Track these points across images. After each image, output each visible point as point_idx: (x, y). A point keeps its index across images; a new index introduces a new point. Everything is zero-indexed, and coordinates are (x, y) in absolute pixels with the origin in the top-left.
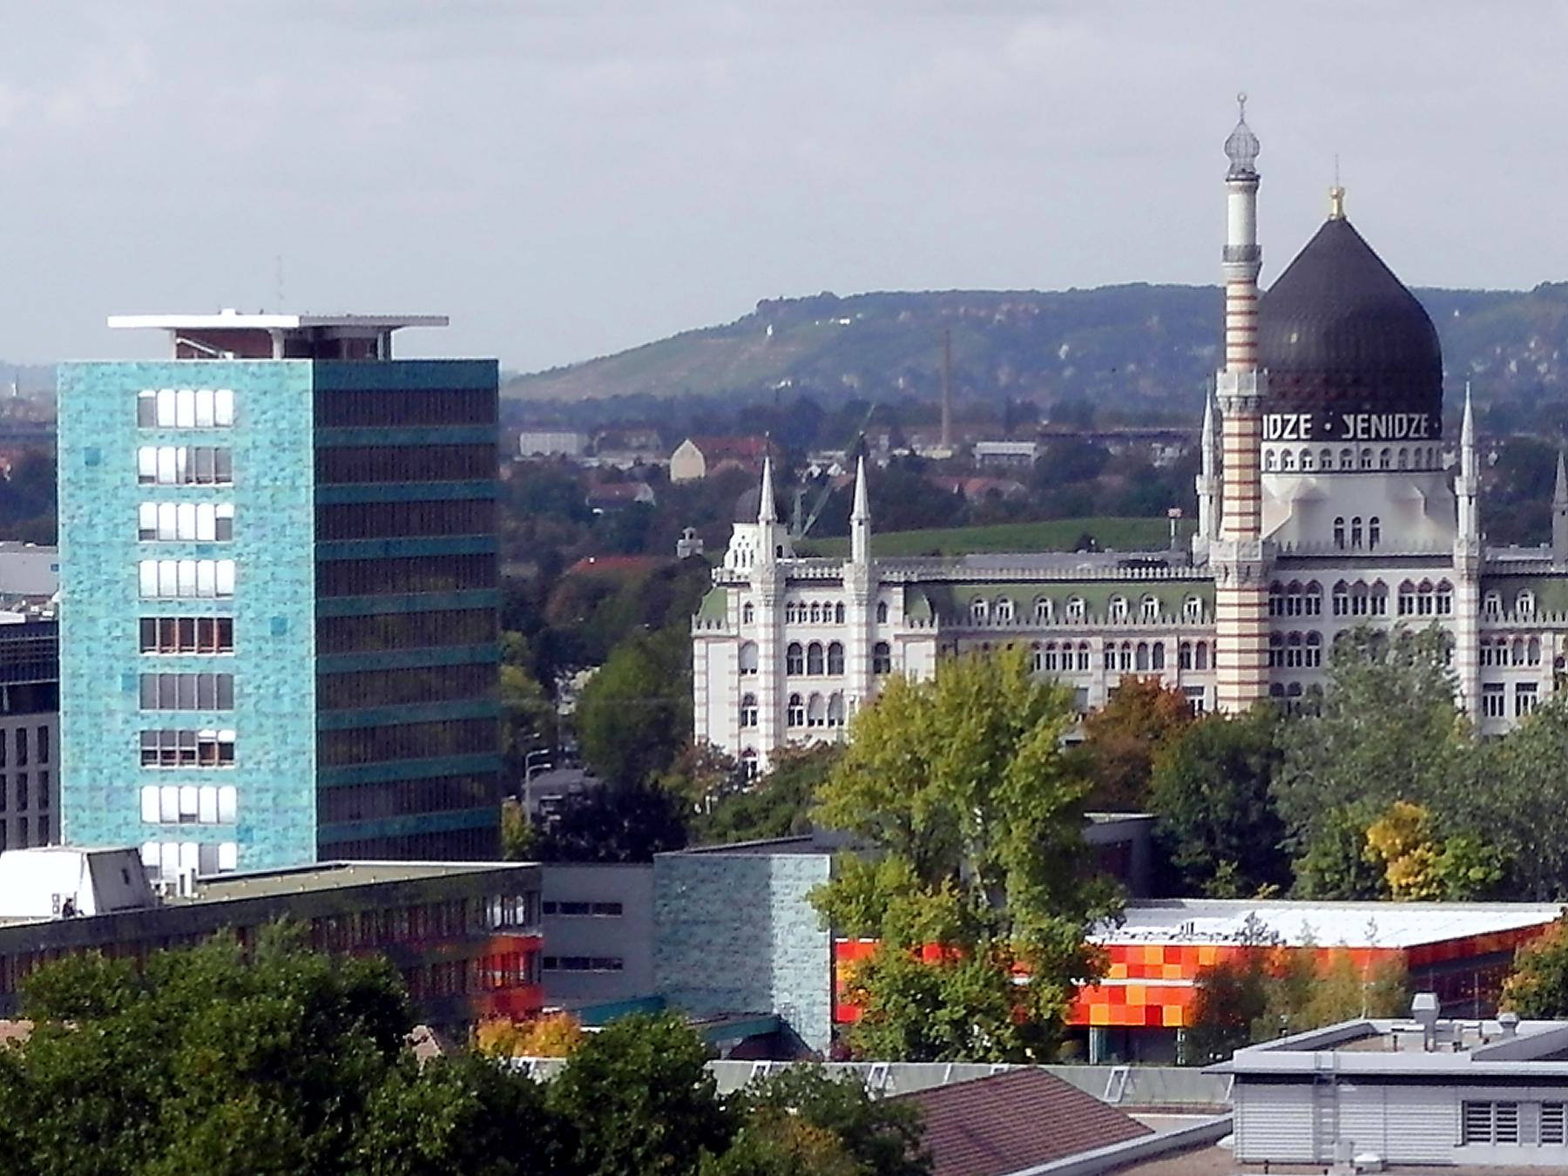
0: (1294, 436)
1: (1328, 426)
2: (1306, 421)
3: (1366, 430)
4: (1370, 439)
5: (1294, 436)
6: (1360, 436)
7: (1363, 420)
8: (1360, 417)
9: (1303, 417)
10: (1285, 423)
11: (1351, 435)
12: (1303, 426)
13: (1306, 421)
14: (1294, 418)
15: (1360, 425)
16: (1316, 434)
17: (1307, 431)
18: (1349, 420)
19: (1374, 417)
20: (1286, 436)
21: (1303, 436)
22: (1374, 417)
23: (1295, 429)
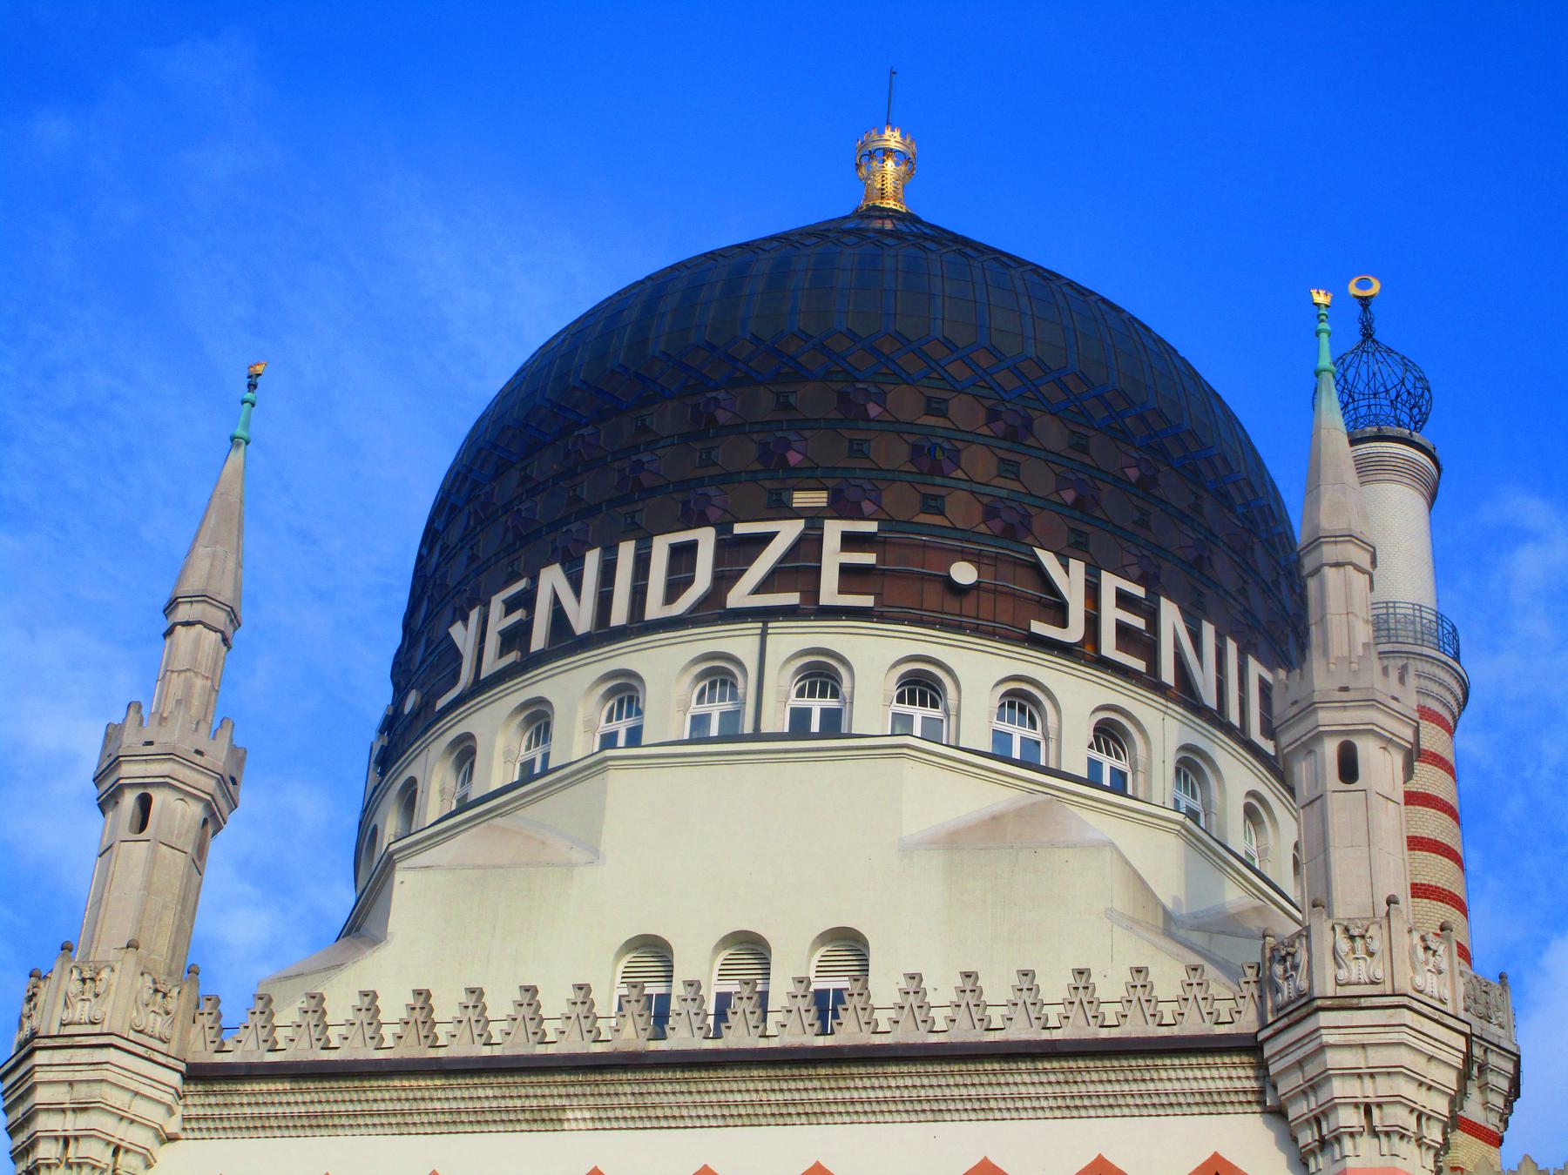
0: (793, 598)
1: (963, 573)
2: (851, 541)
3: (1142, 642)
4: (1150, 681)
5: (793, 598)
6: (1109, 647)
7: (1123, 599)
8: (1110, 583)
11: (1074, 633)
12: (833, 557)
14: (788, 532)
15: (1110, 613)
17: (851, 576)
18: (1070, 581)
19: (1170, 616)
20: (740, 595)
21: (829, 593)
22: (1170, 616)
23: (799, 568)
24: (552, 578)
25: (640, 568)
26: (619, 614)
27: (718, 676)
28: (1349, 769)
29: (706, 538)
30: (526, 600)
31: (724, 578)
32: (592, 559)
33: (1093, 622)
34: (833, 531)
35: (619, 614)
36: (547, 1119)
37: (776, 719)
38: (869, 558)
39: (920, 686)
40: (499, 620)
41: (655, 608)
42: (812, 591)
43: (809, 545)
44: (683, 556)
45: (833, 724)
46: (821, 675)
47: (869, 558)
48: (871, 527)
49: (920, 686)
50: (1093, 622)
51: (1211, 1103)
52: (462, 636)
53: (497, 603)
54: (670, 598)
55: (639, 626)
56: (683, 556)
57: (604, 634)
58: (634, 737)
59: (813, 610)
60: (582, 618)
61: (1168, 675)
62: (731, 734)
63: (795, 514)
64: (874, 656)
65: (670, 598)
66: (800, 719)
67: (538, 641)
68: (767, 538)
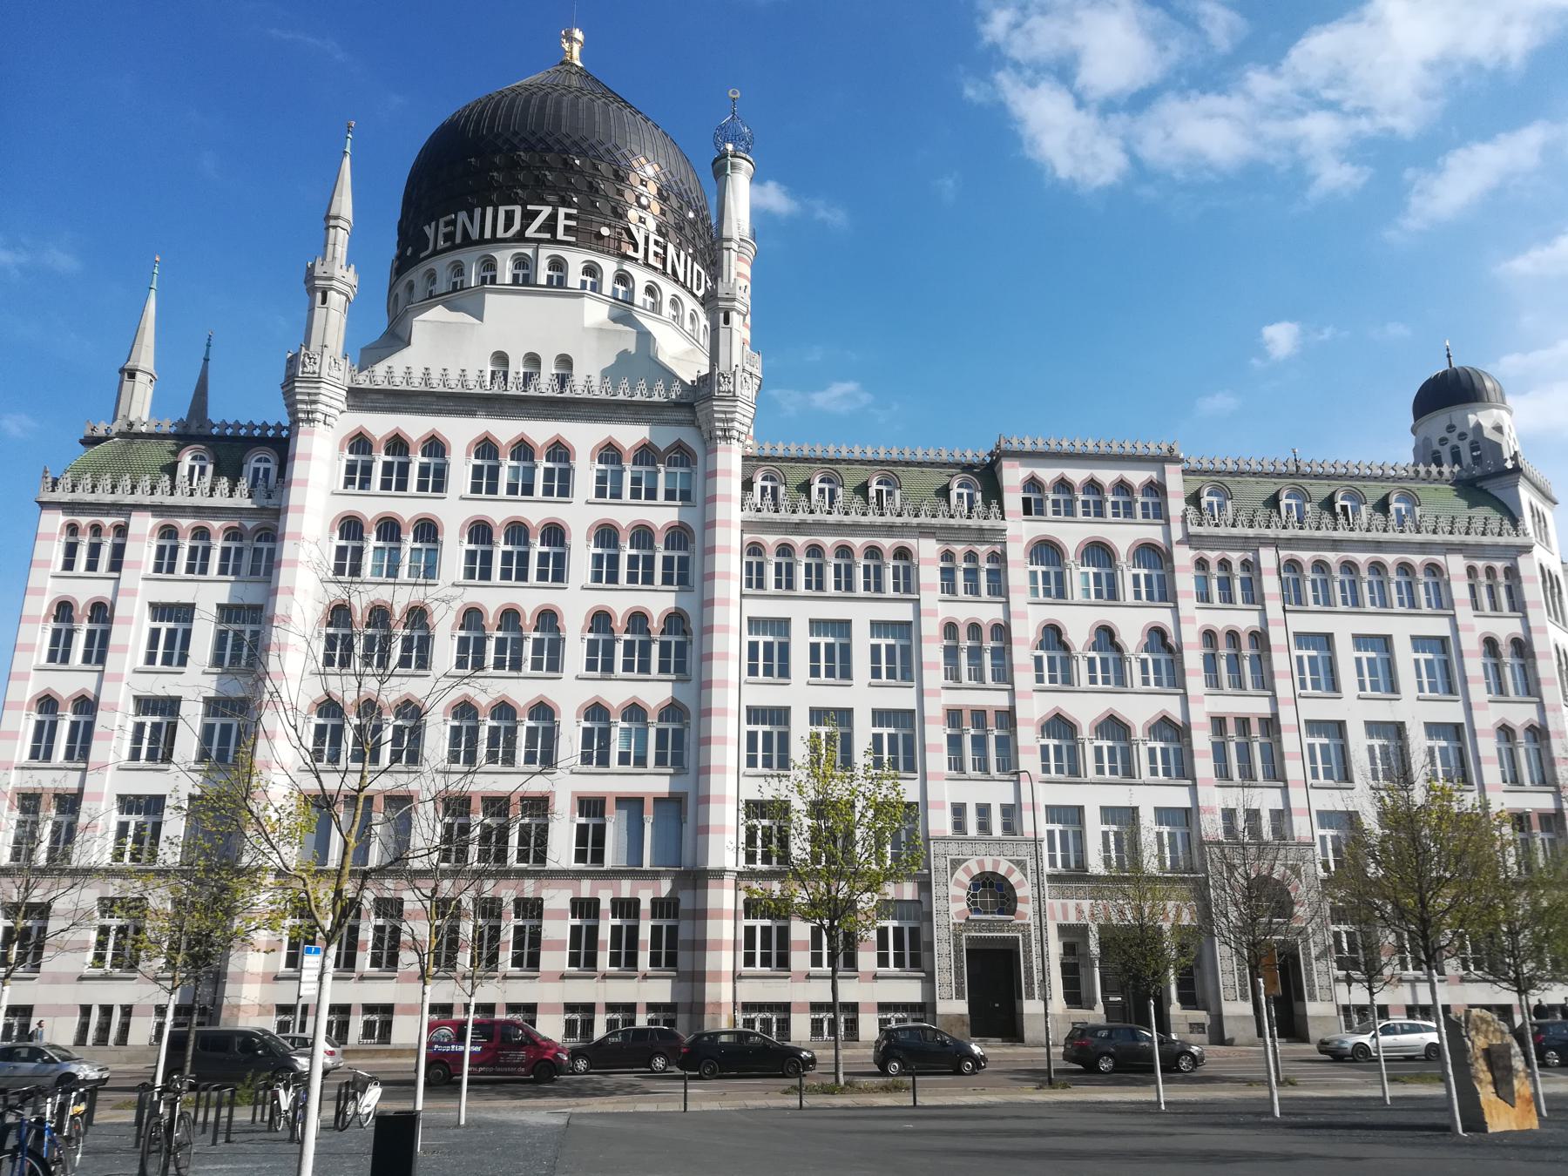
0: (548, 236)
2: (568, 217)
5: (548, 236)
6: (652, 260)
7: (656, 243)
9: (562, 211)
10: (529, 217)
11: (640, 255)
12: (562, 222)
13: (568, 217)
14: (546, 211)
16: (586, 237)
17: (567, 228)
20: (530, 233)
21: (560, 235)
22: (671, 249)
24: (462, 216)
25: (494, 219)
26: (488, 235)
27: (521, 262)
28: (727, 321)
29: (518, 210)
30: (453, 223)
31: (524, 227)
32: (478, 212)
33: (646, 251)
34: (562, 211)
35: (488, 235)
36: (471, 413)
37: (542, 280)
38: (573, 223)
39: (591, 270)
40: (443, 230)
41: (500, 234)
42: (554, 234)
43: (553, 217)
44: (510, 217)
45: (562, 282)
46: (558, 264)
47: (573, 223)
48: (574, 211)
49: (591, 270)
50: (646, 251)
51: (679, 423)
52: (429, 231)
53: (442, 221)
54: (506, 230)
55: (494, 239)
56: (510, 217)
57: (482, 241)
58: (493, 281)
59: (554, 241)
60: (475, 235)
61: (669, 270)
62: (526, 283)
63: (548, 204)
64: (576, 260)
65: (506, 230)
66: (550, 278)
67: (458, 240)
68: (538, 213)
